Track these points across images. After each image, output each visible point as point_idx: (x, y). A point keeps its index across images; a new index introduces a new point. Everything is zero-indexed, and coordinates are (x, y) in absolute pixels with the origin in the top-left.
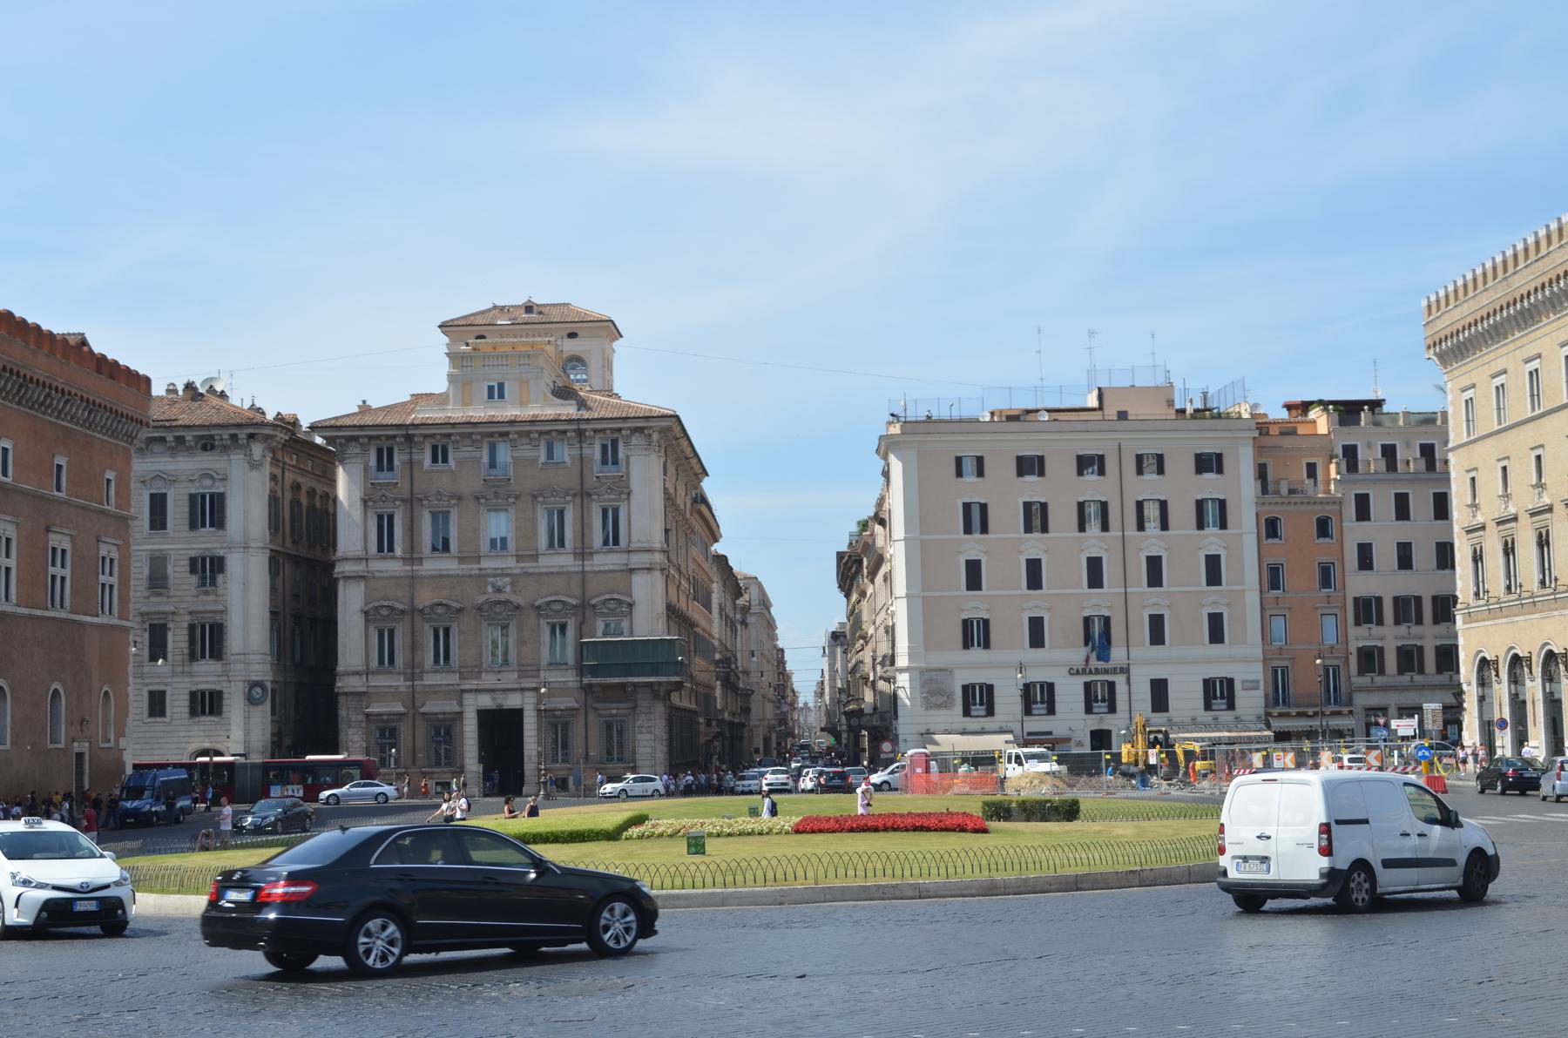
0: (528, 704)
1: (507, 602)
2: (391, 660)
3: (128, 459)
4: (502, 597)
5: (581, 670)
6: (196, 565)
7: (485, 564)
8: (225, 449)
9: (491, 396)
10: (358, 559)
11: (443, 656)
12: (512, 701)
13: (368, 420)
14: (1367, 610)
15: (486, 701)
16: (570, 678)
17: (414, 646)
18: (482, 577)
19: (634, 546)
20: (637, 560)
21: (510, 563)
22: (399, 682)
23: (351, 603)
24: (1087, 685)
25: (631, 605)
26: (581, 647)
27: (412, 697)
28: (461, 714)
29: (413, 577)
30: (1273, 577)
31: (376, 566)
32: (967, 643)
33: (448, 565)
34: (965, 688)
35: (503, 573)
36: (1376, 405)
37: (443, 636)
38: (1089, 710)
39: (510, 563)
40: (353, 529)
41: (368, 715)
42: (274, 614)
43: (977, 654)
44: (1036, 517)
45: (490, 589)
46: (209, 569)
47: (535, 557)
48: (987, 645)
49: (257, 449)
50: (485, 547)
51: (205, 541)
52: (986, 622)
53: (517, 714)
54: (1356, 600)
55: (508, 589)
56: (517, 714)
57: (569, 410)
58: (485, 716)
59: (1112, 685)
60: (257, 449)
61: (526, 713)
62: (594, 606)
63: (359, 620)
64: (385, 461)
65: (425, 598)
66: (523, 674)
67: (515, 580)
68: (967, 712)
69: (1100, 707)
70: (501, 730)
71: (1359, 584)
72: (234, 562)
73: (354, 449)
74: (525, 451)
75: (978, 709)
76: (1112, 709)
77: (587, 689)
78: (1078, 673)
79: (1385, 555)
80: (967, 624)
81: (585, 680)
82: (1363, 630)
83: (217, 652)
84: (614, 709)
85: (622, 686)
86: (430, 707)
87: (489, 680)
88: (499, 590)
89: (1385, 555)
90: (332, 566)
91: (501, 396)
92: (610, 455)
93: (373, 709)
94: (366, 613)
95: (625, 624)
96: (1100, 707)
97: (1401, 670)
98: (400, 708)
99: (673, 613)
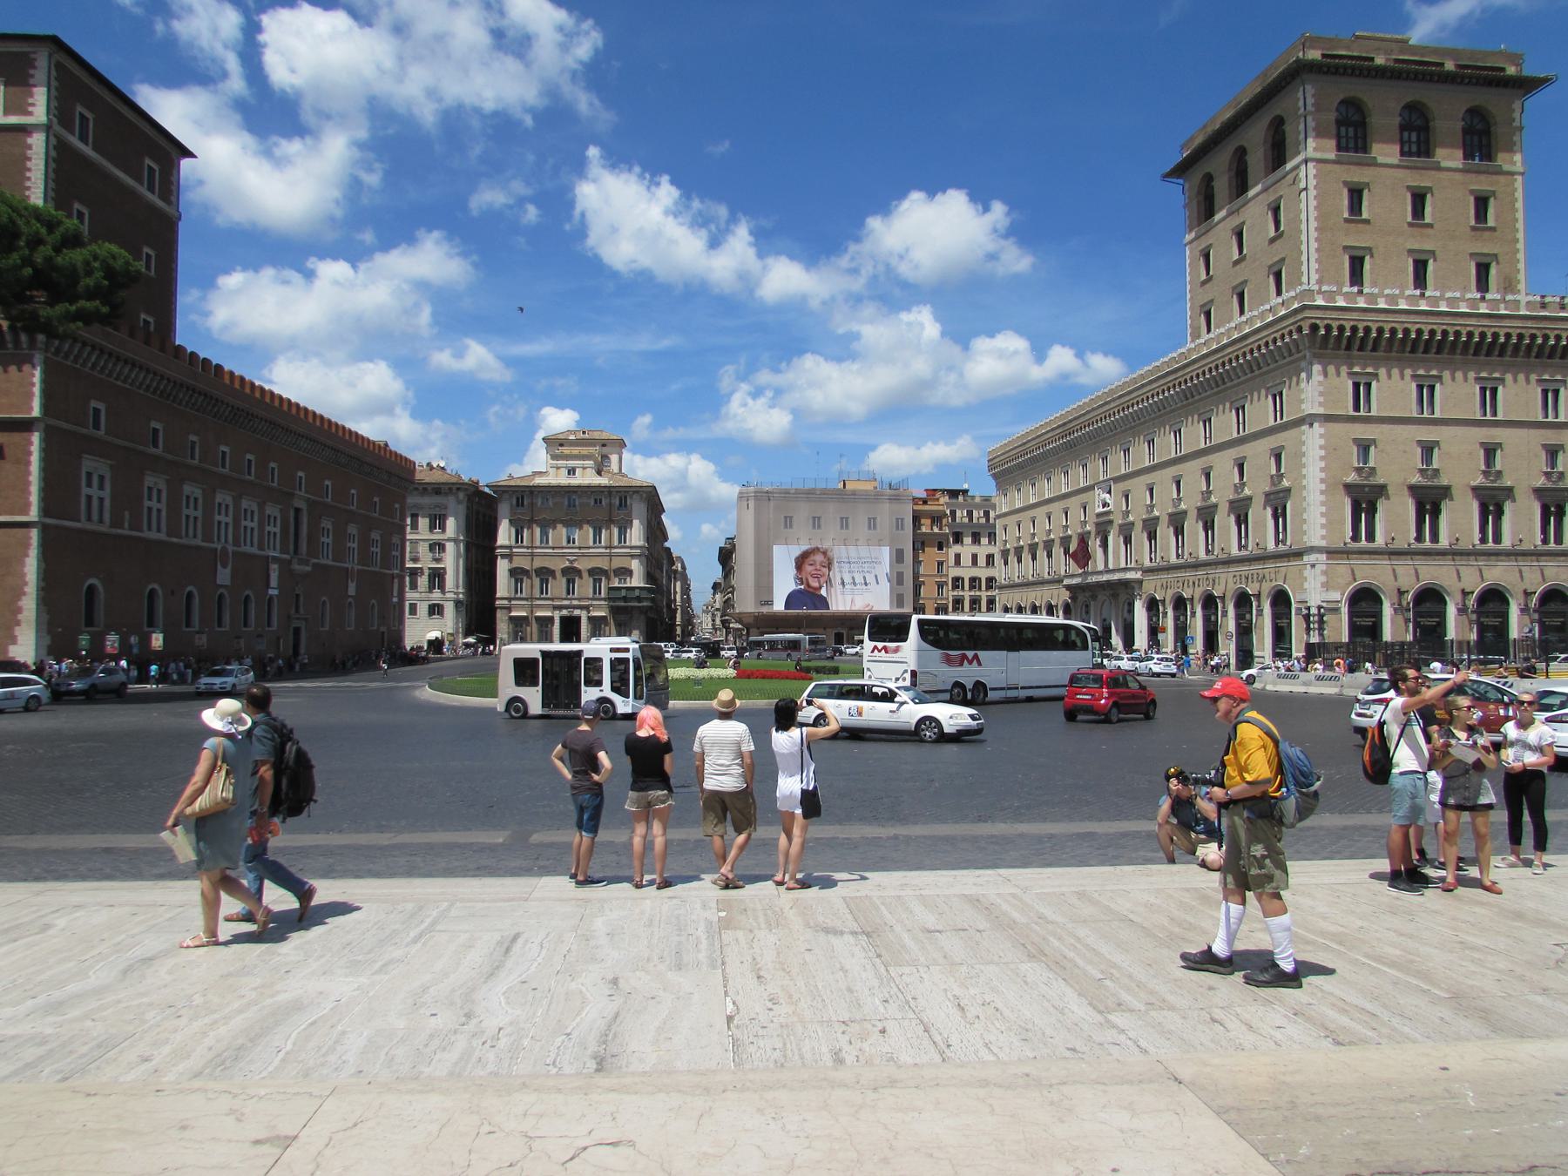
0: (584, 615)
3: (404, 498)
5: (609, 599)
6: (432, 548)
8: (446, 494)
12: (577, 612)
13: (512, 483)
14: (957, 582)
15: (565, 612)
18: (563, 555)
23: (502, 567)
28: (551, 619)
29: (532, 555)
36: (965, 492)
37: (544, 582)
40: (504, 535)
41: (511, 618)
42: (468, 571)
46: (437, 547)
49: (461, 495)
50: (564, 544)
51: (437, 536)
53: (578, 618)
56: (578, 618)
58: (563, 619)
60: (461, 495)
63: (506, 574)
64: (520, 503)
65: (538, 563)
71: (954, 572)
72: (450, 547)
73: (506, 496)
74: (585, 500)
79: (966, 560)
83: (442, 587)
84: (622, 617)
86: (539, 614)
89: (966, 560)
92: (623, 504)
97: (972, 609)
99: (650, 577)
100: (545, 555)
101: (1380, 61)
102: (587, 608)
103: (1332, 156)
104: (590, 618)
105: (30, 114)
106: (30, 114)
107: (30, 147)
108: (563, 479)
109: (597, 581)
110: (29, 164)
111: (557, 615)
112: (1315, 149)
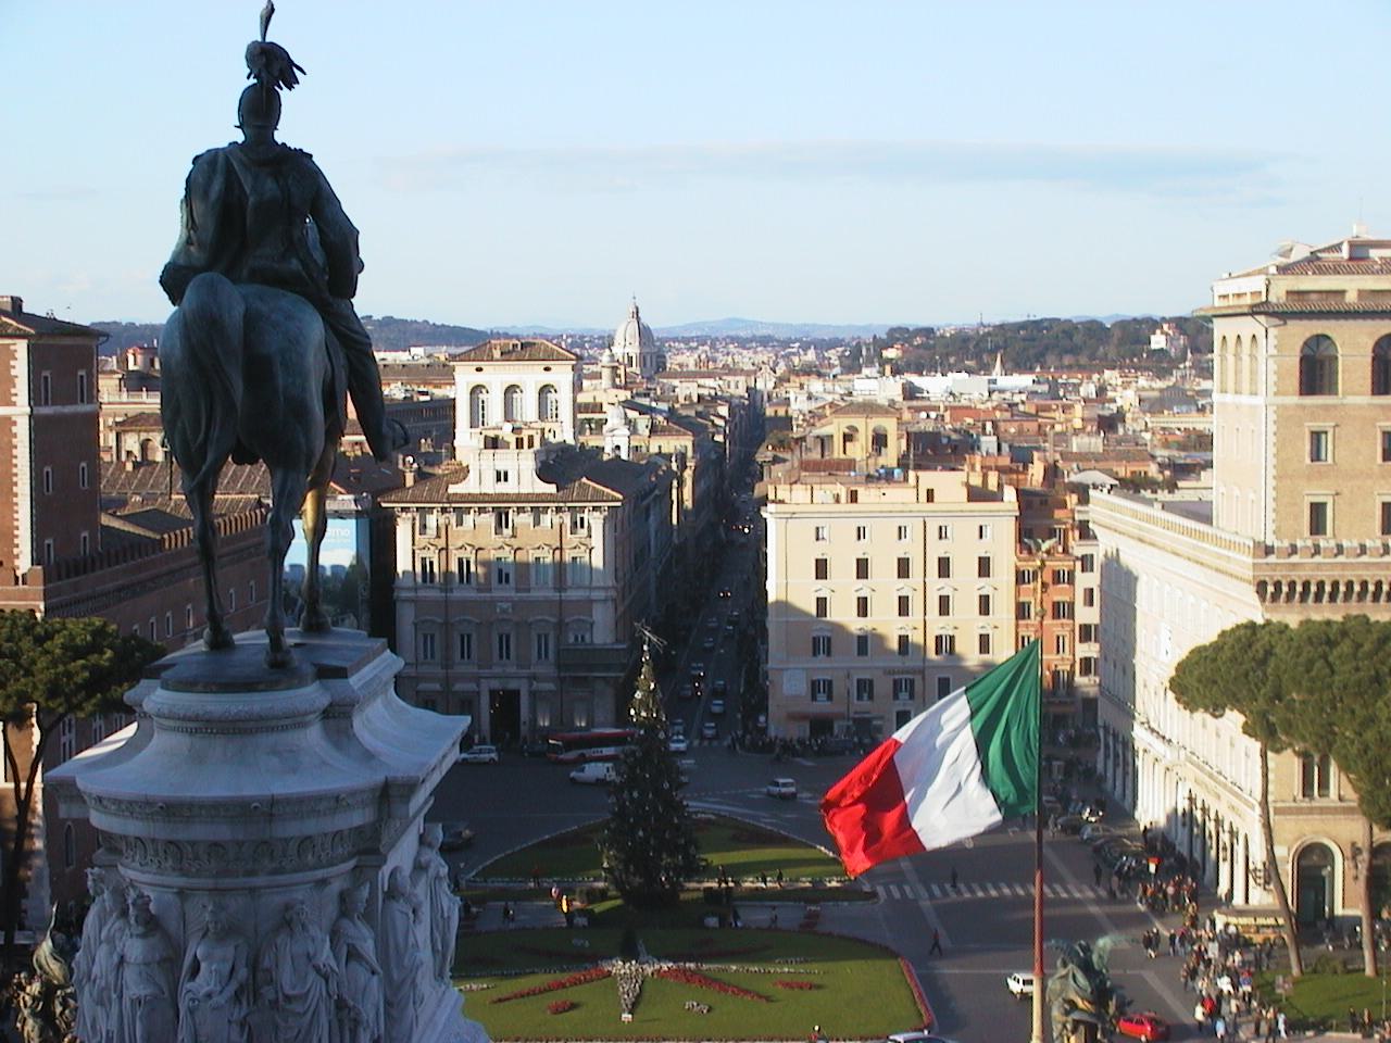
1: (509, 620)
2: (432, 656)
4: (505, 616)
5: (559, 666)
7: (496, 594)
9: (499, 480)
10: (409, 589)
11: (466, 653)
12: (512, 685)
15: (495, 684)
16: (551, 670)
17: (447, 648)
18: (492, 602)
19: (594, 584)
20: (597, 595)
21: (513, 594)
22: (440, 671)
24: (895, 682)
25: (592, 625)
26: (558, 653)
27: (447, 682)
28: (478, 693)
30: (1022, 611)
31: (422, 593)
32: (815, 653)
33: (473, 594)
34: (813, 683)
35: (507, 600)
38: (896, 697)
39: (513, 594)
41: (417, 692)
43: (822, 661)
44: (862, 569)
45: (498, 610)
47: (529, 590)
48: (829, 654)
52: (829, 639)
53: (516, 694)
54: (1080, 626)
55: (510, 610)
56: (516, 694)
57: (552, 489)
58: (493, 693)
59: (912, 682)
61: (522, 693)
62: (567, 624)
66: (519, 666)
67: (515, 604)
68: (814, 698)
69: (904, 695)
70: (506, 702)
75: (822, 697)
76: (912, 697)
77: (562, 680)
78: (889, 673)
80: (816, 641)
81: (562, 674)
82: (1085, 646)
85: (586, 678)
86: (458, 687)
87: (497, 670)
88: (504, 611)
90: (393, 591)
91: (506, 480)
93: (422, 686)
94: (415, 624)
95: (587, 637)
96: (904, 695)
98: (437, 687)
100: (464, 603)
101: (1351, 297)
102: (534, 677)
103: (1295, 399)
104: (533, 694)
105: (14, 404)
106: (14, 404)
107: (15, 436)
108: (491, 487)
109: (542, 639)
110: (15, 452)
111: (485, 687)
112: (1275, 394)
